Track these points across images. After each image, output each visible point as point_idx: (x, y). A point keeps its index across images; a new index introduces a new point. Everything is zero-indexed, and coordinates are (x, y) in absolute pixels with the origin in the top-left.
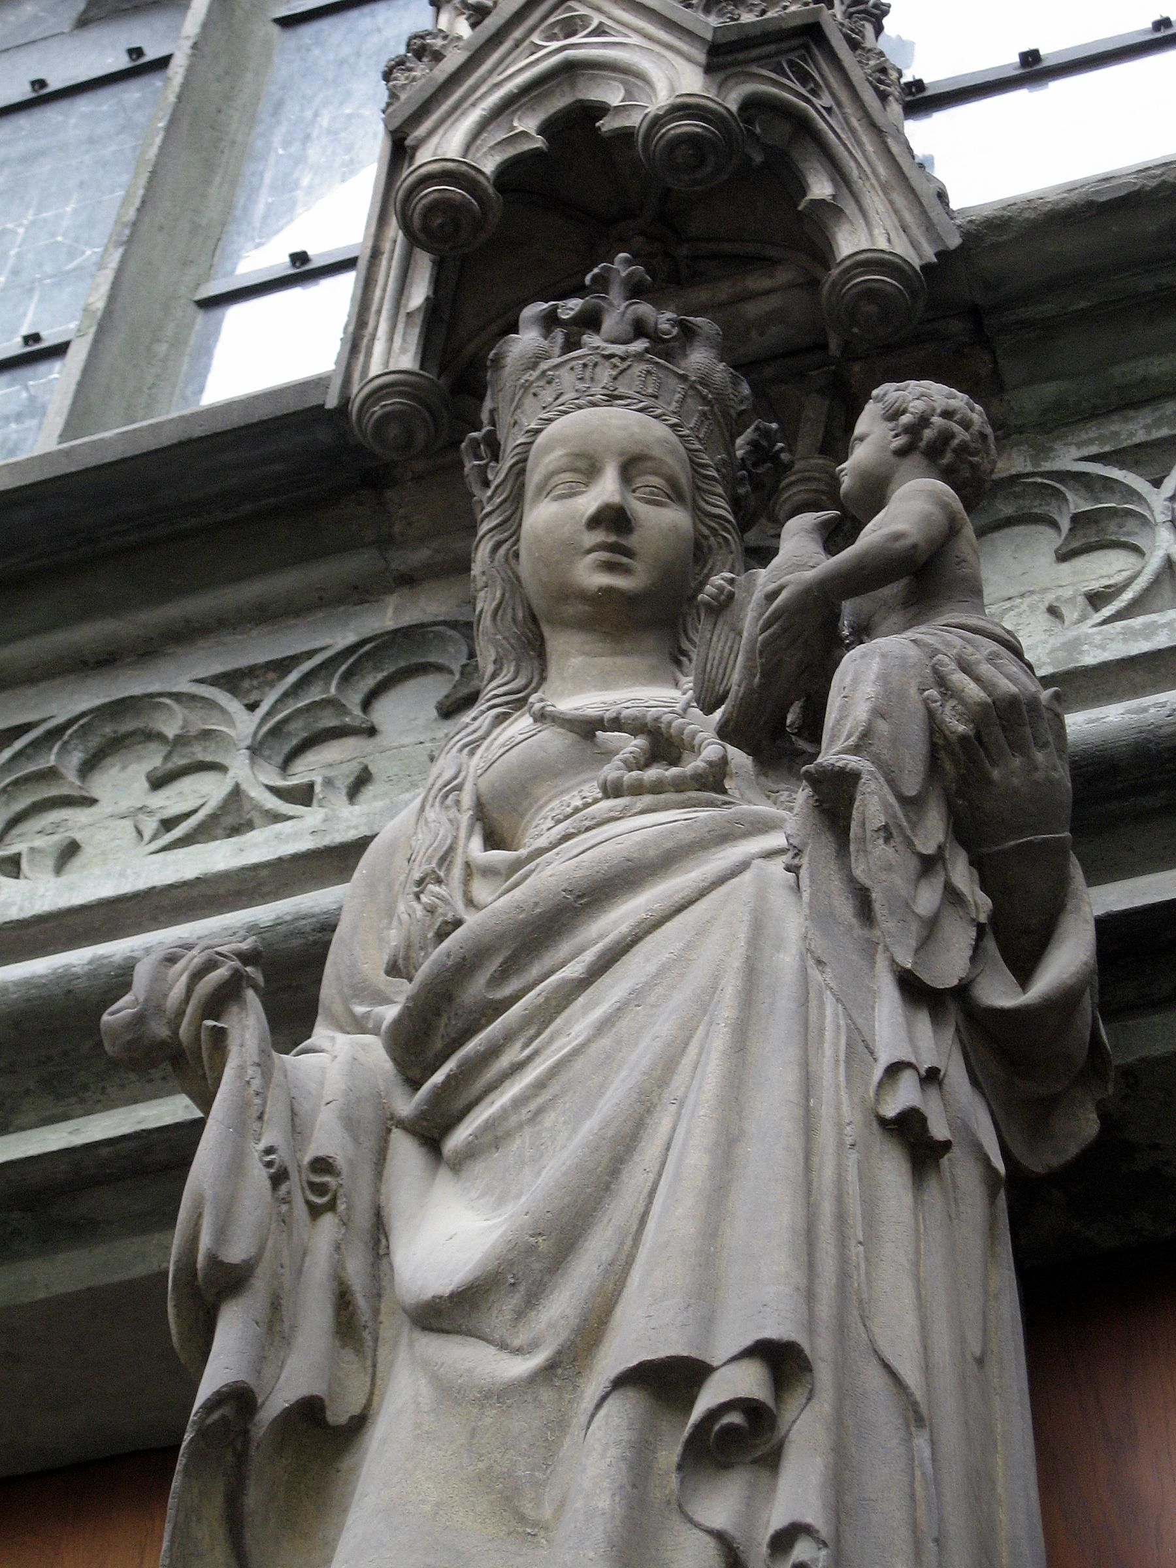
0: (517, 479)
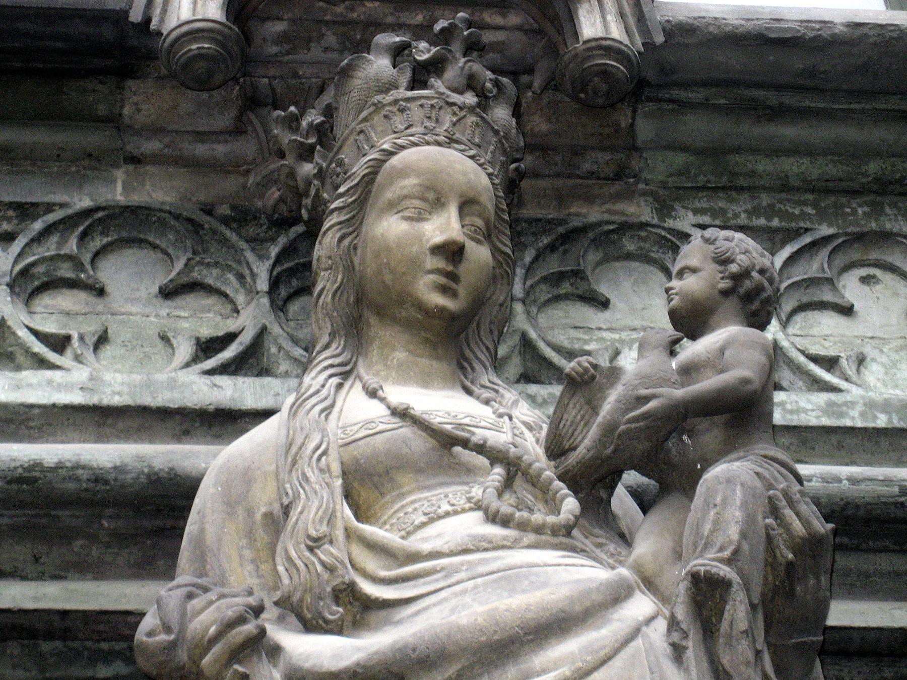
0: (366, 186)
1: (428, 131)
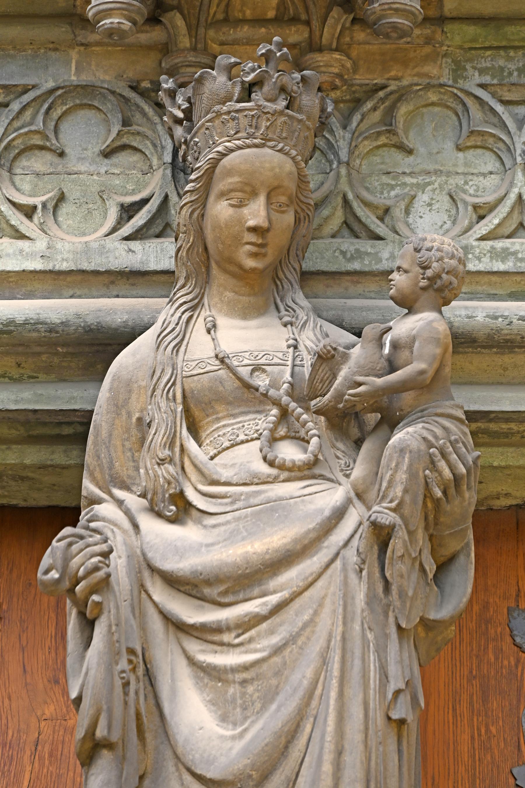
1: (250, 136)
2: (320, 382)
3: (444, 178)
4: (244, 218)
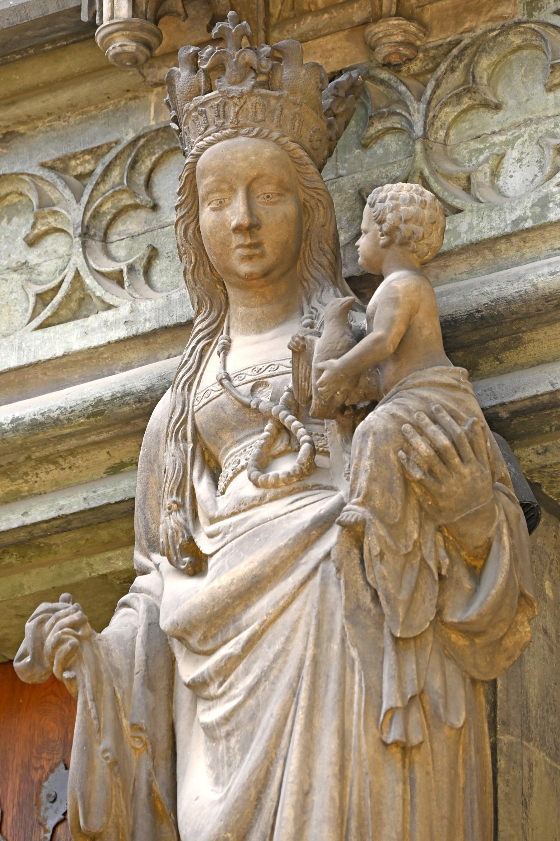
0: (191, 183)
1: (221, 127)
2: (305, 380)
3: (533, 127)
4: (227, 220)
